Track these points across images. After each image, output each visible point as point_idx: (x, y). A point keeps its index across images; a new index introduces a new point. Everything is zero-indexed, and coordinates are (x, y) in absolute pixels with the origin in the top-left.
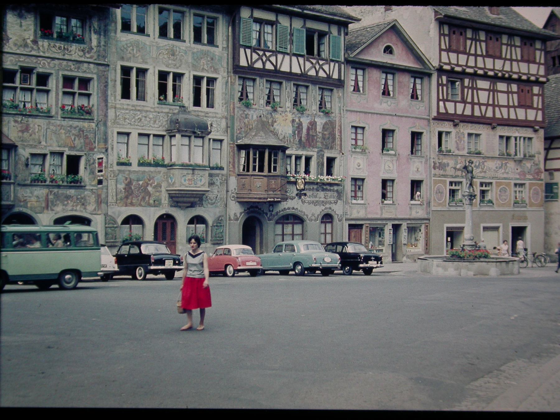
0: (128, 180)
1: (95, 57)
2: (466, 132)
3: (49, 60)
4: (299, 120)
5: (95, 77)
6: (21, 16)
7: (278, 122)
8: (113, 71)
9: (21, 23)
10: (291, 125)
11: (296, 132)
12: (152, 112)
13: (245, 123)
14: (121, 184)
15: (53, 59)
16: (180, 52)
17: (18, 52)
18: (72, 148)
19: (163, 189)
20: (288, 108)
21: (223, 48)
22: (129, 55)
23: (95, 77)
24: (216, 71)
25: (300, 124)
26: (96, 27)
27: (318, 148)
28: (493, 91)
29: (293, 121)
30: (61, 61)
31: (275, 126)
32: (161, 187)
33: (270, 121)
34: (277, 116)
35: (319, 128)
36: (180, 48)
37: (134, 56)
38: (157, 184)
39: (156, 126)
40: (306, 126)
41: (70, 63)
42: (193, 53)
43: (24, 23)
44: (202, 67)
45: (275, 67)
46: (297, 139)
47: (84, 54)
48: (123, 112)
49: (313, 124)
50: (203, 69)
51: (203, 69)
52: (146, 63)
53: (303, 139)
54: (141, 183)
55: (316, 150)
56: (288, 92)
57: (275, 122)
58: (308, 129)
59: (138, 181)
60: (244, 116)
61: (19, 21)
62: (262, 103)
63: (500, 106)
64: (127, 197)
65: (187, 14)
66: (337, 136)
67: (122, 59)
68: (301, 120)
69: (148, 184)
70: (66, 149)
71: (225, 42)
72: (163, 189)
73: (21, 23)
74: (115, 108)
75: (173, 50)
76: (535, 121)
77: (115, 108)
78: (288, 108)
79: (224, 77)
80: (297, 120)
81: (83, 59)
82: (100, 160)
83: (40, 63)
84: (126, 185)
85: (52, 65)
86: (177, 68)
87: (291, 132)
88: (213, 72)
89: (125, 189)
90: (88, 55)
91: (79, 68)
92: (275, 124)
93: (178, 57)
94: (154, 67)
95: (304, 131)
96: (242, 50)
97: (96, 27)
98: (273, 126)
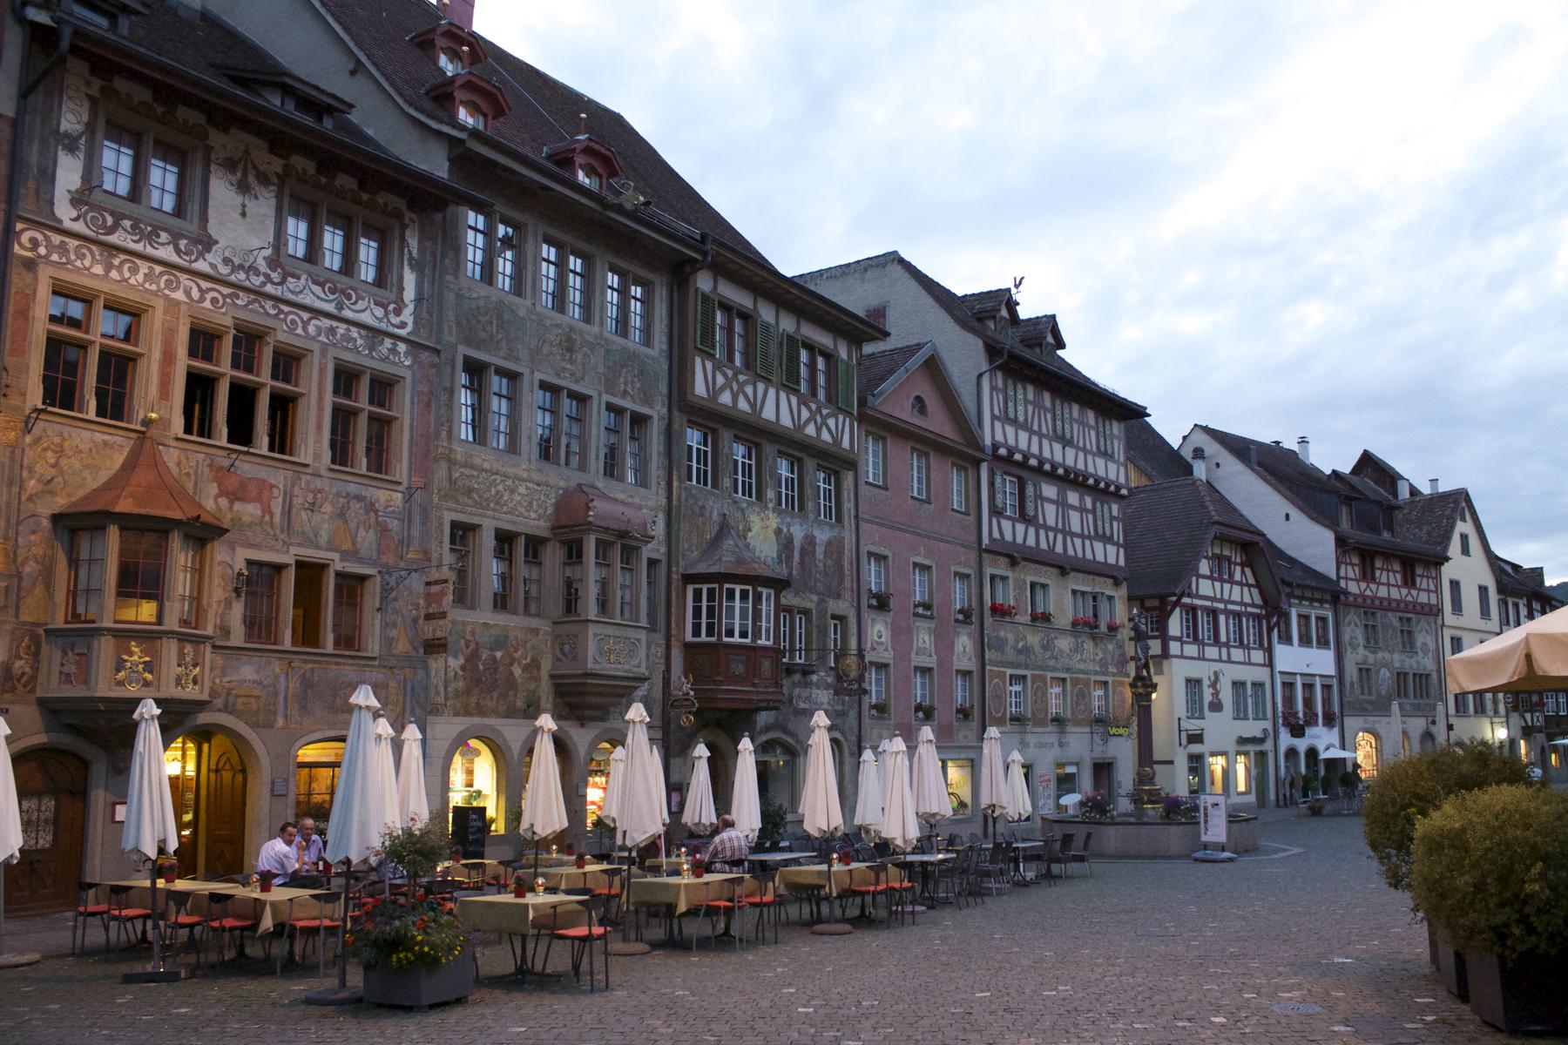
0: (472, 646)
1: (410, 328)
2: (1029, 579)
3: (306, 316)
5: (408, 374)
6: (243, 188)
7: (755, 530)
8: (448, 369)
9: (244, 206)
12: (524, 480)
14: (456, 657)
15: (317, 313)
17: (232, 278)
18: (351, 555)
19: (544, 674)
21: (661, 351)
22: (482, 335)
23: (408, 374)
24: (648, 401)
25: (790, 540)
26: (415, 252)
27: (818, 594)
28: (1062, 504)
29: (778, 532)
30: (335, 324)
32: (539, 668)
35: (820, 554)
37: (492, 337)
38: (533, 660)
39: (533, 515)
41: (354, 332)
42: (608, 352)
43: (252, 206)
45: (753, 405)
47: (387, 314)
48: (467, 471)
49: (810, 541)
50: (625, 393)
52: (517, 360)
54: (498, 654)
55: (815, 598)
58: (803, 549)
59: (492, 649)
60: (697, 509)
61: (238, 200)
63: (1074, 535)
64: (468, 692)
65: (598, 262)
67: (468, 342)
68: (792, 529)
69: (512, 661)
70: (336, 556)
71: (664, 339)
72: (544, 674)
73: (244, 206)
74: (449, 460)
75: (569, 339)
76: (1116, 567)
77: (449, 460)
79: (661, 418)
81: (383, 326)
82: (435, 589)
83: (285, 320)
84: (467, 660)
85: (311, 329)
86: (576, 381)
89: (463, 668)
90: (395, 320)
91: (372, 348)
95: (796, 555)
96: (698, 361)
97: (415, 252)
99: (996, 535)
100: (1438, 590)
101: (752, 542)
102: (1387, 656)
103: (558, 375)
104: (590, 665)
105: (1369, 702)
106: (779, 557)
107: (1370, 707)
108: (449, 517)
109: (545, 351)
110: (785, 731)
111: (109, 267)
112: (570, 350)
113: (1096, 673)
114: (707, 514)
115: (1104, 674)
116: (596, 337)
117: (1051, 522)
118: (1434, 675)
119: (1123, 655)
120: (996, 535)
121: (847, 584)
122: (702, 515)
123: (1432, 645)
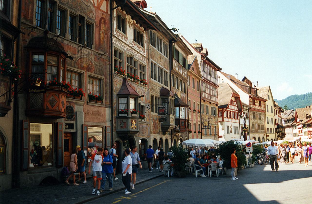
63: (211, 95)
99: (202, 96)
100: (265, 107)
102: (257, 121)
104: (170, 124)
105: (254, 131)
107: (254, 132)
108: (151, 94)
111: (119, 44)
113: (215, 125)
115: (215, 125)
117: (209, 93)
118: (264, 125)
119: (218, 121)
120: (202, 96)
123: (264, 119)
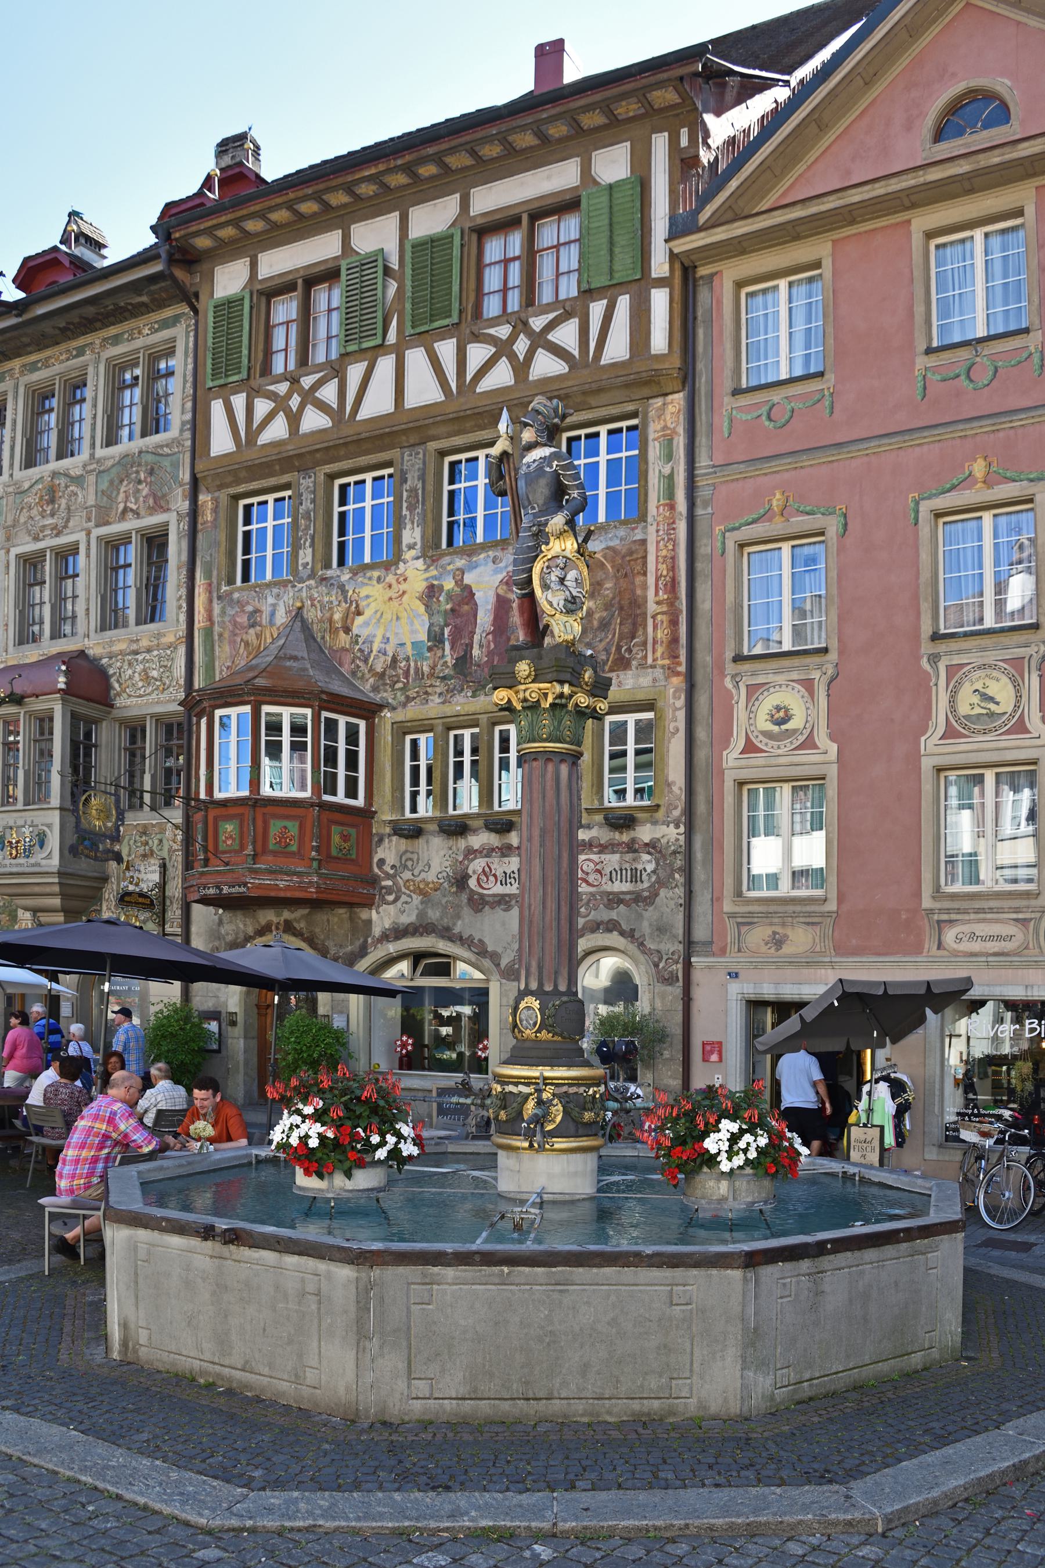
4: (459, 582)
7: (368, 613)
10: (422, 609)
11: (447, 631)
13: (247, 644)
16: (67, 487)
20: (411, 547)
25: (467, 595)
29: (432, 592)
31: (355, 630)
33: (337, 616)
34: (364, 592)
36: (66, 475)
40: (492, 599)
44: (121, 506)
46: (449, 655)
51: (125, 510)
53: (476, 652)
56: (413, 491)
57: (359, 613)
60: (243, 619)
62: (309, 559)
66: (652, 607)
68: (468, 579)
78: (411, 547)
80: (449, 584)
87: (423, 636)
88: (152, 511)
92: (359, 620)
93: (63, 502)
94: (8, 552)
95: (485, 618)
98: (347, 630)
101: (364, 633)
103: (36, 539)
106: (436, 639)
109: (22, 520)
110: (446, 933)
112: (52, 501)
114: (265, 619)
116: (85, 466)
121: (656, 631)
122: (252, 626)
